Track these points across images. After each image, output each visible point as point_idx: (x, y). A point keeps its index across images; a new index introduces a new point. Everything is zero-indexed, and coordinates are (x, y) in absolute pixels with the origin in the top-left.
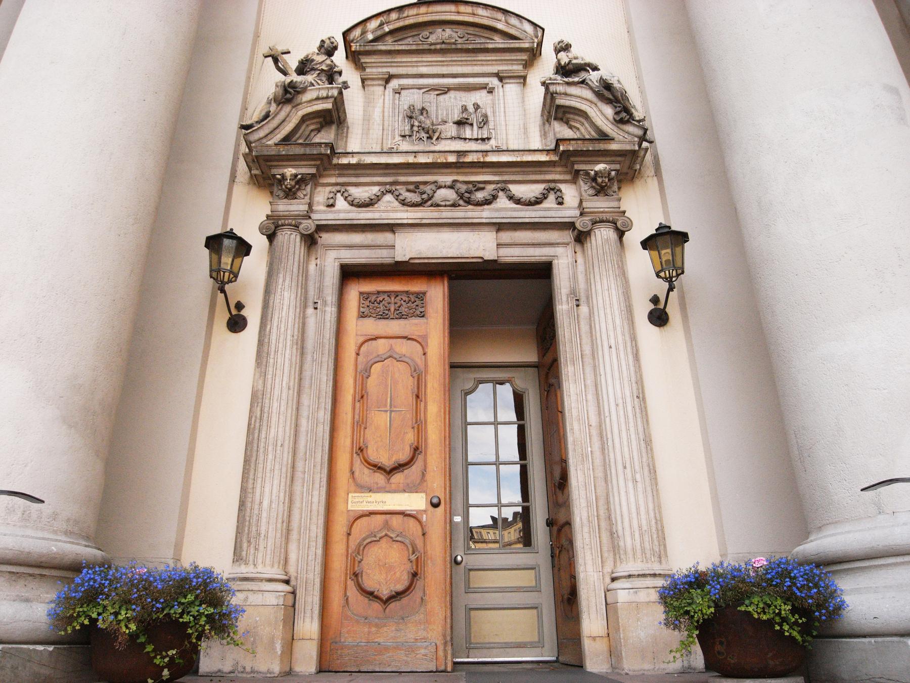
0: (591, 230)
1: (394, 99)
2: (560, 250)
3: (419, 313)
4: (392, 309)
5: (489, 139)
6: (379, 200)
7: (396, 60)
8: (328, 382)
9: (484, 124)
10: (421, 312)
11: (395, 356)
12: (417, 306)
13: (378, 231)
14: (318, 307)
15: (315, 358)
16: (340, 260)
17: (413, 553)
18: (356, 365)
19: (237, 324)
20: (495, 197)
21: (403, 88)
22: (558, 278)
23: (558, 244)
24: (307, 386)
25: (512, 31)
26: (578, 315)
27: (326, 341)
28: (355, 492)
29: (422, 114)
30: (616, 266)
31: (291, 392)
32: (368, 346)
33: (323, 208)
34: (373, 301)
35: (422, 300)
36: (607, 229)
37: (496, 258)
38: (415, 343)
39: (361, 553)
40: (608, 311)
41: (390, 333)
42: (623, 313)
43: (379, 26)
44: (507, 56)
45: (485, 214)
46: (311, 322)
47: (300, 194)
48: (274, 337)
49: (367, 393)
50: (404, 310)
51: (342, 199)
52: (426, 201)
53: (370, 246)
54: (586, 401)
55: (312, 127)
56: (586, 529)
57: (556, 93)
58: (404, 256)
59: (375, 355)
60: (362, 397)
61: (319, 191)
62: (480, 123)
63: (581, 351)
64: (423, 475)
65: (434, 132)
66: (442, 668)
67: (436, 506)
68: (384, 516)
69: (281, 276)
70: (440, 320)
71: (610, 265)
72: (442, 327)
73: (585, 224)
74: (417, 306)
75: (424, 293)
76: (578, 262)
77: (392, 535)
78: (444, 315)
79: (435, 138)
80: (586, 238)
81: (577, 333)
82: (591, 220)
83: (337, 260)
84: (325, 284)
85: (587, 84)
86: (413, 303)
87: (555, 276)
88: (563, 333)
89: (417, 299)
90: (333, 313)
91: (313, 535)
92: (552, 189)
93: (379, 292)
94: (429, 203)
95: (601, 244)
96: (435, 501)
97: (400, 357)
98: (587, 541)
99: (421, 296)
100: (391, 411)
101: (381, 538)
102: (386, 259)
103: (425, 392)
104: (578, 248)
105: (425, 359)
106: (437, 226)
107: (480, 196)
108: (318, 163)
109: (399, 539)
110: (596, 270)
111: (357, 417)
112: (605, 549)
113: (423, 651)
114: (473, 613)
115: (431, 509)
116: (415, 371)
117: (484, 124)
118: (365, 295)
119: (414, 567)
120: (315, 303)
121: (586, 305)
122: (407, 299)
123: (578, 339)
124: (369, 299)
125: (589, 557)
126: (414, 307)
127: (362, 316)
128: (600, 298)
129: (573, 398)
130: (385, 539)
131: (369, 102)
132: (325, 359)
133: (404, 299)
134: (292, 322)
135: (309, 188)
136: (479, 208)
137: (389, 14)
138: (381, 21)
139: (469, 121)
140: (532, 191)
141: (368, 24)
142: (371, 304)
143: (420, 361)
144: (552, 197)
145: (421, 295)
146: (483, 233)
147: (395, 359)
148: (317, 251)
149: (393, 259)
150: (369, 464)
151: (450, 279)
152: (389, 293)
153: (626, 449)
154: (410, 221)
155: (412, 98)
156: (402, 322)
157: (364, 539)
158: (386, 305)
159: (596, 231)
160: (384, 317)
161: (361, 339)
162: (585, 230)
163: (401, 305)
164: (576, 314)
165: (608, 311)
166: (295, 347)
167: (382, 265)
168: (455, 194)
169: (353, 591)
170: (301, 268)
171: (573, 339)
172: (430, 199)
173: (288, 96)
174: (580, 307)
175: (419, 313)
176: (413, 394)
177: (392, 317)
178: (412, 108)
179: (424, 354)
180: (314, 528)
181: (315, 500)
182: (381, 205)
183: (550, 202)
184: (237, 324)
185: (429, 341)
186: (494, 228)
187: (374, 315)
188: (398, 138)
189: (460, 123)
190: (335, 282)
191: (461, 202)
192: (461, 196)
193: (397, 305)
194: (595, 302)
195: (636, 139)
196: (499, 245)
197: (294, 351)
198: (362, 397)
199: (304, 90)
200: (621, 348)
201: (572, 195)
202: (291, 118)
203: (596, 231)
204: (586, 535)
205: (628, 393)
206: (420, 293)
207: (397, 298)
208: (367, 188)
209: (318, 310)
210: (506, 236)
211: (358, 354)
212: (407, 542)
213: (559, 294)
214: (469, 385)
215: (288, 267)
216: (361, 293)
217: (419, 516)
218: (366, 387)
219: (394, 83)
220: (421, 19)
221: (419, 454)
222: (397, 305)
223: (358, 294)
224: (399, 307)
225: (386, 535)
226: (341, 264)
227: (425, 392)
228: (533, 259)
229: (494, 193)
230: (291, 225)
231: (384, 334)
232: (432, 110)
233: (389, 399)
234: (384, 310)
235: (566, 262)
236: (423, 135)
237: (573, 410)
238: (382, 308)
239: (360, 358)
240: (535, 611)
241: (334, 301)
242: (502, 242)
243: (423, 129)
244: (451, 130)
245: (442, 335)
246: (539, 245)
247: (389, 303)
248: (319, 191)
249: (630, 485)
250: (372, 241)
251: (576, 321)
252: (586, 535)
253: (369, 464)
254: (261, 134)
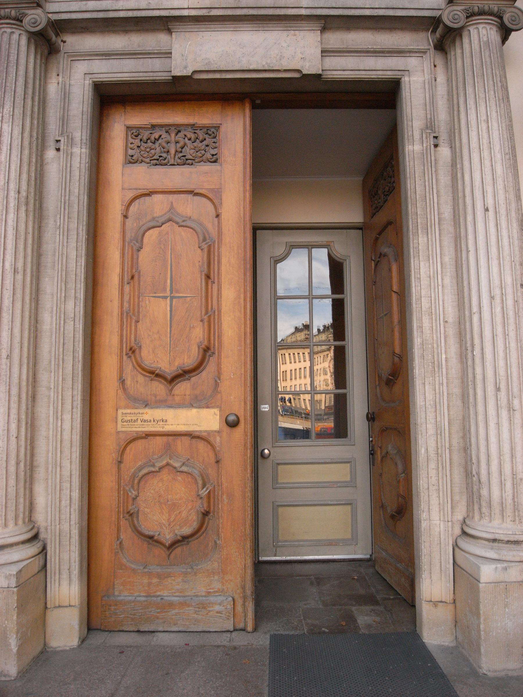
0: (462, 28)
2: (412, 62)
3: (209, 156)
4: (173, 151)
8: (79, 259)
10: (213, 155)
11: (177, 219)
12: (207, 146)
13: (147, 30)
14: (62, 148)
15: (58, 224)
16: (93, 76)
17: (204, 486)
18: (124, 232)
22: (409, 103)
23: (410, 52)
24: (49, 265)
26: (435, 160)
27: (74, 199)
28: (127, 407)
30: (499, 85)
31: (20, 277)
32: (139, 204)
34: (145, 139)
35: (215, 137)
36: (488, 27)
37: (320, 72)
38: (204, 200)
39: (136, 487)
40: (486, 153)
41: (169, 185)
42: (507, 157)
49: (139, 272)
50: (189, 152)
53: (135, 54)
54: (443, 286)
56: (432, 465)
58: (186, 67)
59: (149, 217)
60: (133, 277)
63: (439, 214)
64: (217, 385)
66: (242, 625)
67: (233, 425)
68: (165, 439)
70: (239, 167)
71: (491, 83)
72: (241, 175)
73: (456, 17)
74: (207, 146)
75: (217, 128)
76: (438, 80)
77: (177, 465)
78: (245, 160)
80: (454, 42)
81: (435, 187)
82: (466, 10)
84: (71, 113)
86: (201, 142)
87: (404, 100)
88: (412, 187)
89: (207, 136)
90: (83, 156)
91: (66, 473)
93: (154, 127)
95: (478, 50)
96: (232, 418)
97: (184, 221)
98: (434, 480)
100: (172, 298)
101: (161, 468)
102: (160, 74)
103: (219, 270)
104: (439, 61)
105: (219, 222)
106: (234, 21)
109: (184, 469)
110: (470, 90)
111: (126, 305)
112: (456, 490)
113: (217, 608)
114: (280, 509)
115: (226, 429)
116: (204, 240)
118: (134, 131)
119: (205, 505)
120: (58, 141)
121: (447, 145)
122: (193, 136)
123: (435, 195)
124: (140, 137)
125: (434, 501)
126: (203, 147)
127: (131, 161)
128: (473, 134)
129: (425, 282)
130: (165, 471)
132: (73, 225)
133: (189, 136)
134: (16, 170)
142: (143, 144)
143: (211, 228)
145: (213, 130)
146: (302, 33)
147: (177, 223)
148: (59, 63)
149: (169, 74)
150: (143, 369)
151: (254, 107)
152: (167, 128)
153: (501, 363)
154: (193, 13)
156: (186, 170)
157: (140, 469)
158: (164, 144)
159: (471, 29)
161: (130, 195)
162: (456, 26)
163: (185, 145)
164: (433, 158)
165: (486, 153)
166: (23, 209)
167: (154, 83)
169: (127, 535)
170: (30, 86)
171: (427, 194)
174: (438, 148)
175: (211, 157)
176: (201, 275)
177: (172, 162)
179: (218, 216)
180: (66, 463)
181: (67, 426)
185: (224, 197)
186: (317, 25)
187: (148, 160)
190: (85, 109)
193: (179, 145)
194: (465, 140)
196: (325, 52)
197: (23, 214)
198: (133, 277)
200: (503, 211)
203: (471, 29)
204: (433, 473)
205: (508, 280)
206: (212, 127)
207: (180, 135)
209: (61, 152)
211: (126, 217)
212: (196, 472)
213: (410, 129)
214: (280, 251)
215: (8, 84)
216: (128, 128)
217: (211, 439)
218: (137, 263)
221: (210, 356)
222: (179, 145)
223: (123, 128)
224: (182, 148)
225: (168, 464)
226: (94, 82)
227: (219, 270)
228: (373, 75)
233: (169, 281)
234: (161, 152)
235: (421, 79)
237: (423, 299)
238: (158, 149)
239: (129, 222)
240: (349, 508)
241: (84, 138)
242: (329, 47)
245: (242, 189)
246: (383, 52)
247: (168, 142)
249: (504, 414)
250: (139, 46)
251: (433, 169)
252: (433, 473)
253: (143, 369)
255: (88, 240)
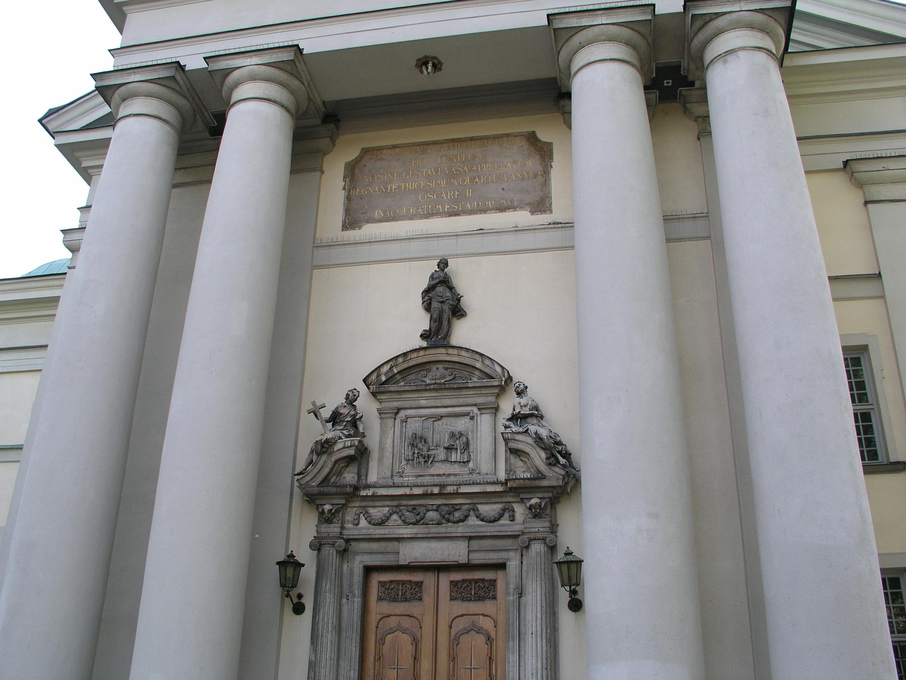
1: (402, 427)
2: (512, 554)
3: (418, 597)
5: (468, 461)
6: (388, 519)
7: (402, 397)
9: (465, 450)
19: (299, 609)
20: (466, 517)
21: (407, 417)
25: (487, 370)
27: (355, 623)
29: (421, 442)
31: (332, 661)
32: (384, 621)
33: (350, 526)
43: (390, 368)
44: (484, 391)
45: (460, 529)
46: (345, 609)
47: (335, 520)
48: (320, 626)
51: (364, 518)
52: (419, 521)
55: (342, 465)
57: (508, 439)
58: (406, 560)
60: (380, 658)
61: (349, 512)
62: (462, 450)
65: (429, 456)
69: (324, 581)
75: (422, 582)
79: (430, 462)
82: (528, 538)
83: (361, 563)
85: (529, 433)
92: (508, 510)
93: (391, 582)
94: (422, 521)
99: (419, 584)
105: (421, 631)
107: (457, 514)
108: (346, 496)
117: (465, 450)
124: (385, 587)
127: (380, 599)
131: (383, 432)
132: (354, 636)
133: (408, 587)
135: (341, 513)
136: (456, 525)
137: (396, 359)
138: (391, 365)
139: (455, 447)
140: (494, 510)
141: (381, 369)
144: (507, 515)
152: (398, 582)
154: (409, 536)
155: (414, 426)
156: (406, 604)
159: (532, 545)
160: (394, 600)
161: (380, 617)
168: (439, 515)
172: (422, 519)
173: (324, 449)
178: (415, 436)
179: (421, 628)
182: (390, 523)
183: (504, 521)
184: (299, 609)
188: (404, 462)
189: (449, 449)
191: (444, 521)
192: (444, 517)
195: (561, 477)
199: (335, 442)
200: (539, 634)
201: (521, 513)
202: (326, 463)
207: (404, 586)
208: (380, 509)
210: (475, 544)
211: (377, 627)
216: (380, 582)
219: (402, 414)
220: (420, 361)
224: (405, 593)
229: (466, 513)
230: (329, 544)
231: (394, 613)
232: (429, 436)
235: (515, 563)
236: (422, 460)
237: (510, 672)
238: (393, 594)
243: (421, 455)
244: (441, 454)
248: (349, 512)
254: (308, 478)
255: (360, 642)
